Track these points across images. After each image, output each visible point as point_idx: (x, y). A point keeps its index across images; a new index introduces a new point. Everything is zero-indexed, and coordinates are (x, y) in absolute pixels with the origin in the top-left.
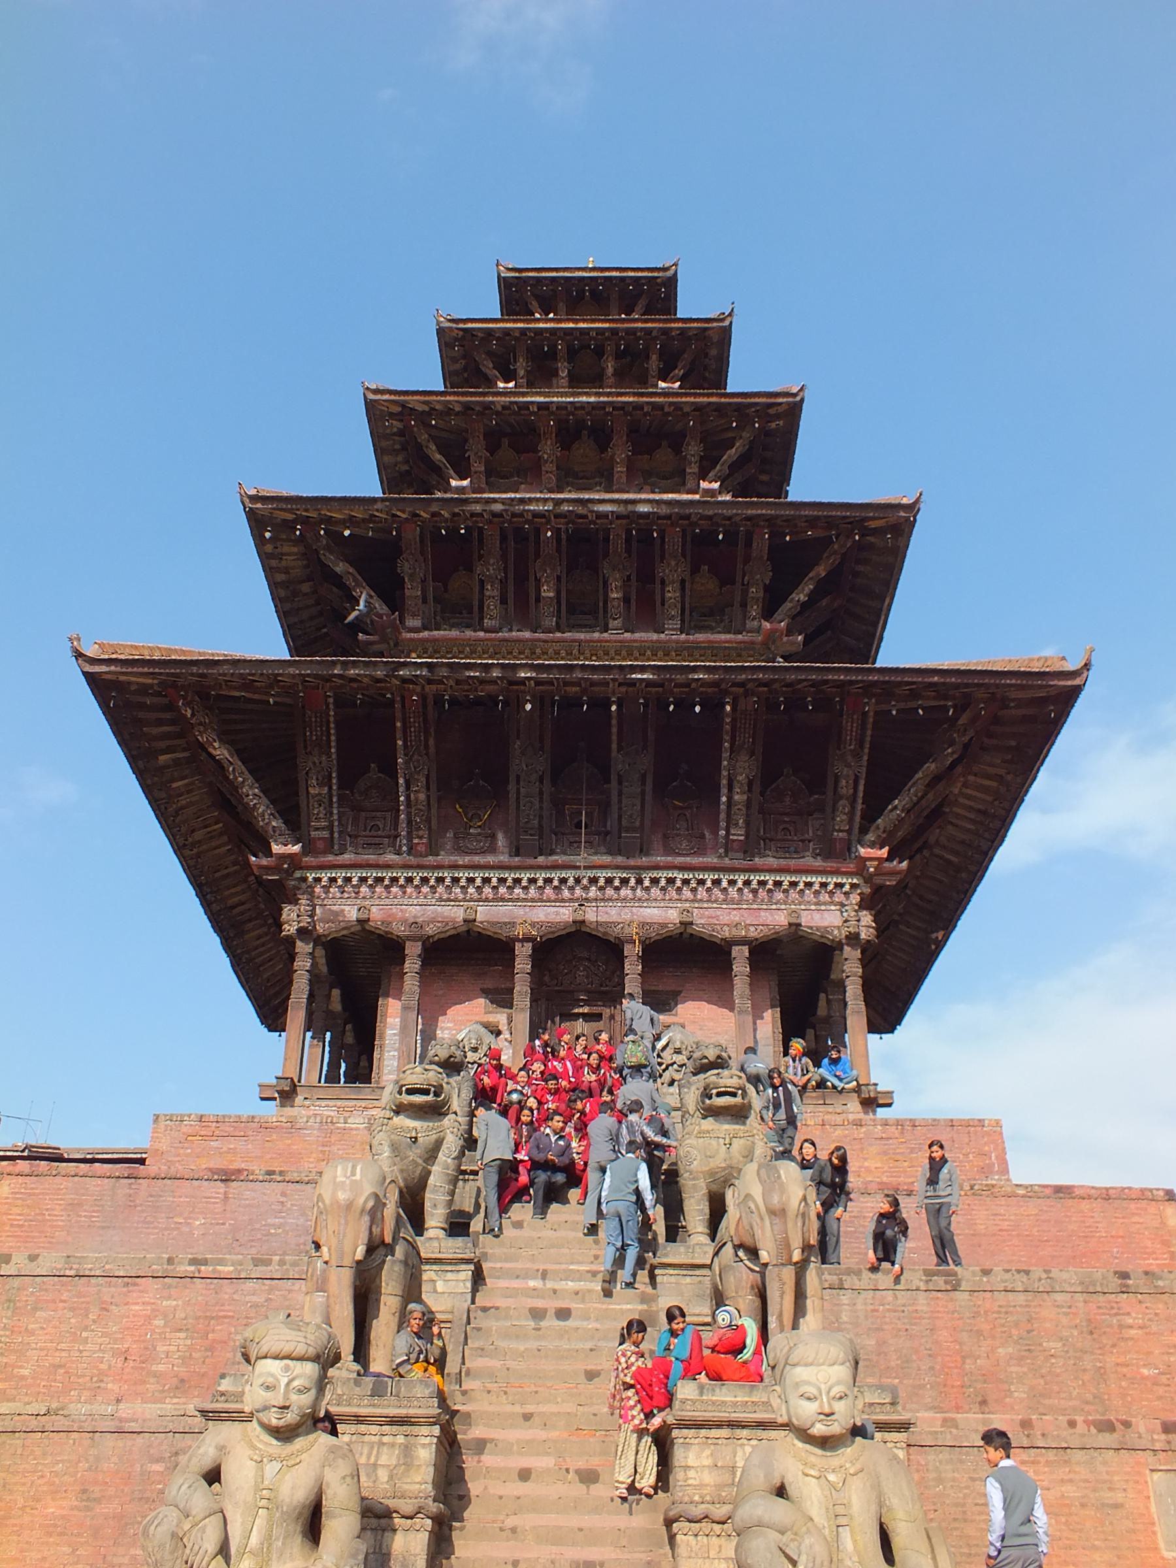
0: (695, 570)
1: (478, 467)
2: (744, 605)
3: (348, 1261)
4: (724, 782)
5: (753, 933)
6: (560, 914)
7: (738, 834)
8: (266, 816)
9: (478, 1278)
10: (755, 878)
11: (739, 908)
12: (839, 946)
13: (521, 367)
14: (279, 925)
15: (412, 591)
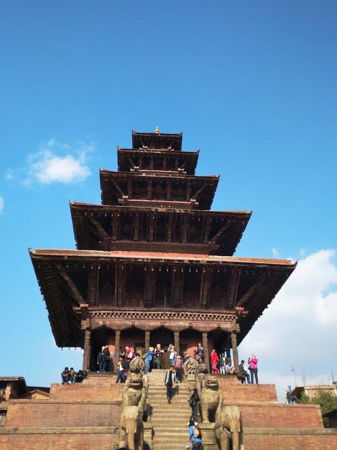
0: (191, 226)
1: (130, 192)
2: (204, 235)
3: (133, 433)
4: (202, 289)
5: (208, 330)
6: (157, 324)
7: (204, 303)
8: (78, 295)
9: (153, 433)
10: (209, 315)
11: (204, 323)
12: (230, 333)
13: (140, 162)
14: (81, 326)
15: (115, 230)
